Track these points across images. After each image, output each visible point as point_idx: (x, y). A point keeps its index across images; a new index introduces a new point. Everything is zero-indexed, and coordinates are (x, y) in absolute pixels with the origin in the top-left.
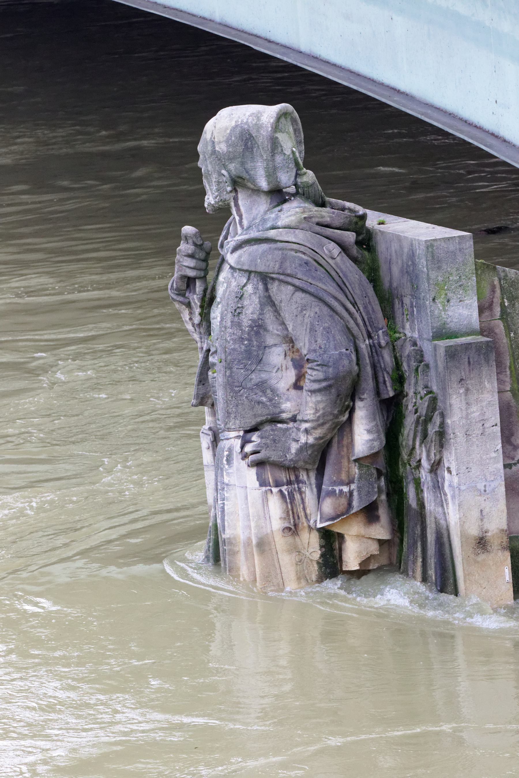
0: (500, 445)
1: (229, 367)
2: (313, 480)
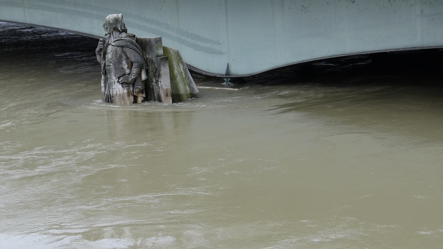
0: (169, 77)
1: (115, 65)
2: (132, 86)
